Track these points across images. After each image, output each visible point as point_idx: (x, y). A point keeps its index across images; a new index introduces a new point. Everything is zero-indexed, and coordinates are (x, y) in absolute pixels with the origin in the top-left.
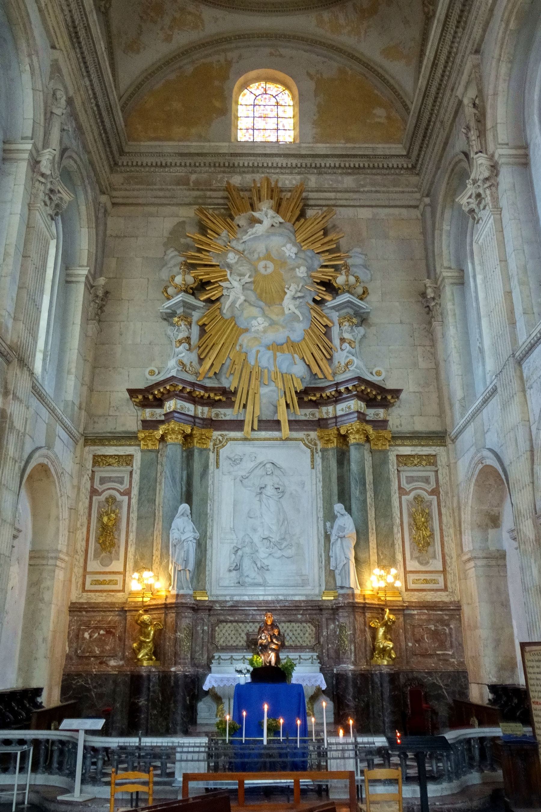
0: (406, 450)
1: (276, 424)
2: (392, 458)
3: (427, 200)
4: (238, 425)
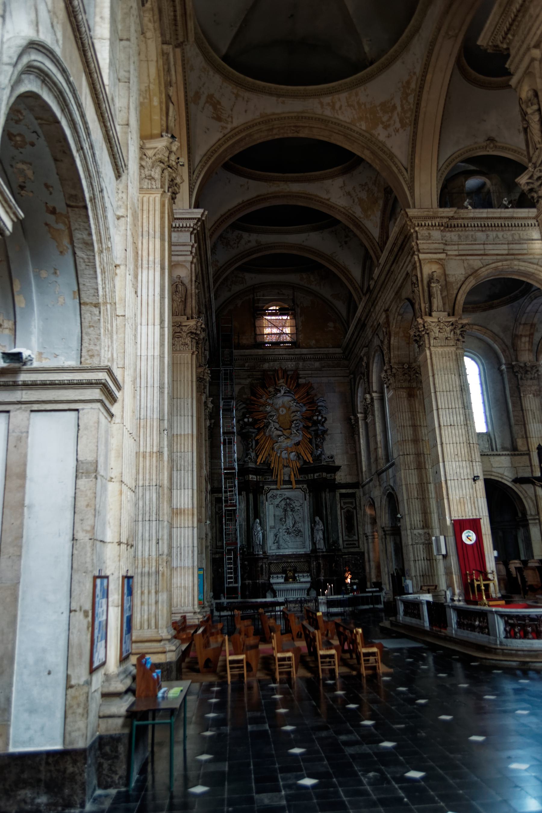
0: (343, 491)
1: (290, 483)
2: (338, 495)
3: (352, 376)
4: (275, 483)
